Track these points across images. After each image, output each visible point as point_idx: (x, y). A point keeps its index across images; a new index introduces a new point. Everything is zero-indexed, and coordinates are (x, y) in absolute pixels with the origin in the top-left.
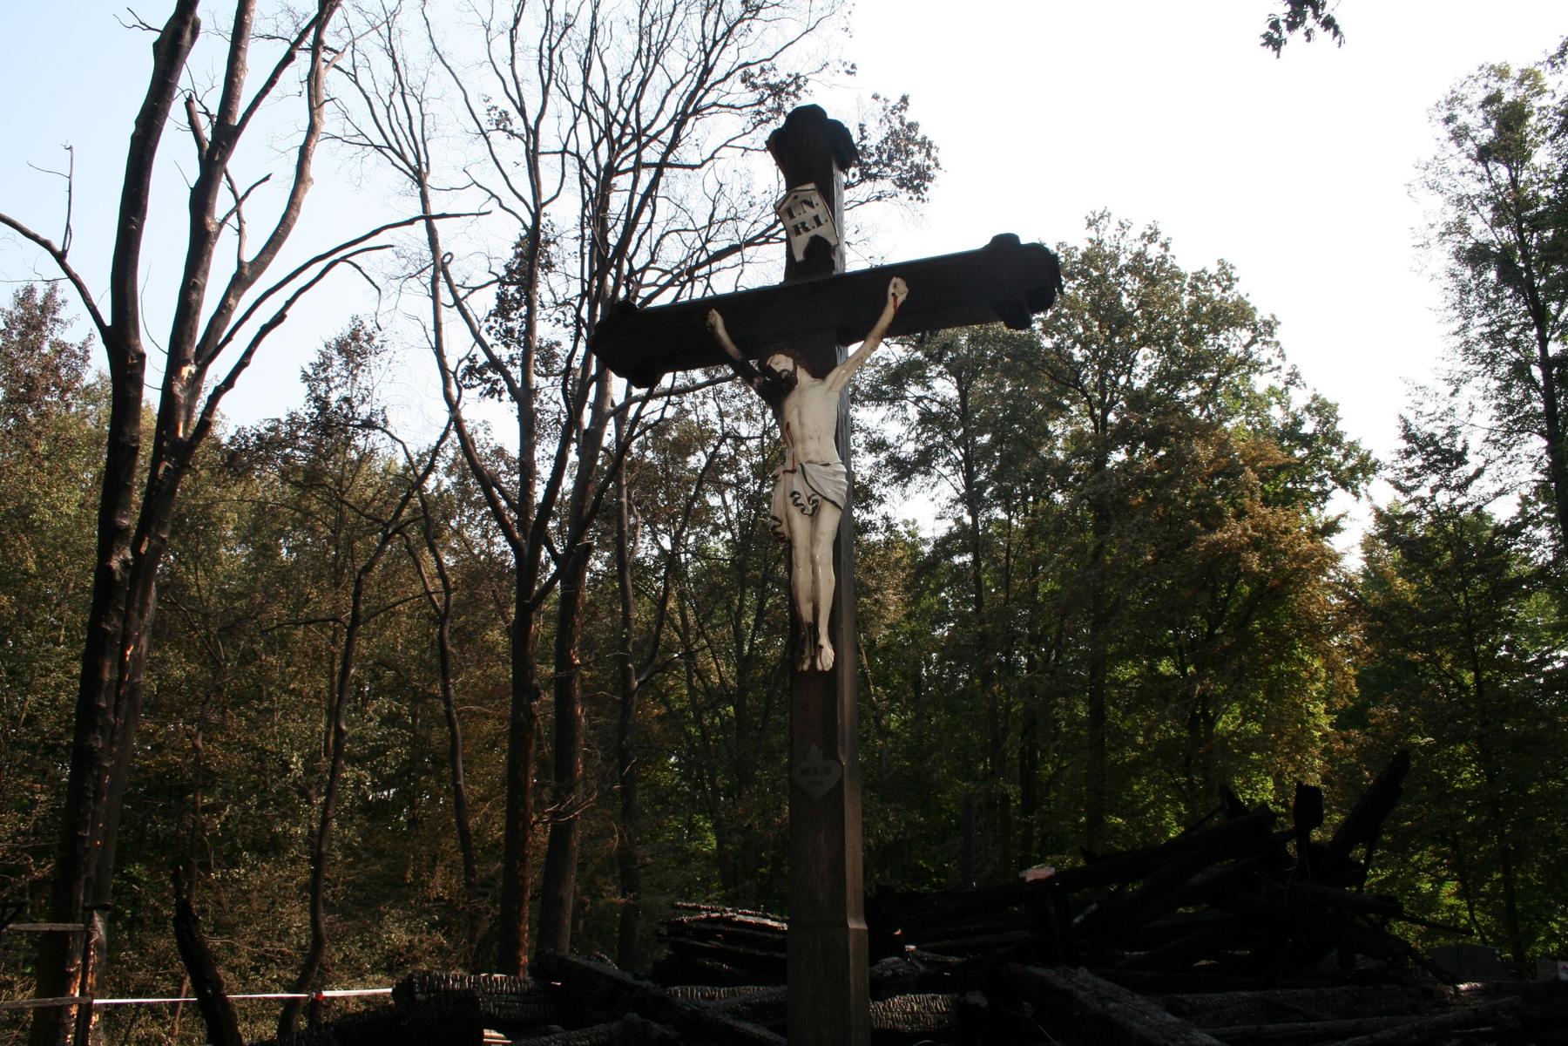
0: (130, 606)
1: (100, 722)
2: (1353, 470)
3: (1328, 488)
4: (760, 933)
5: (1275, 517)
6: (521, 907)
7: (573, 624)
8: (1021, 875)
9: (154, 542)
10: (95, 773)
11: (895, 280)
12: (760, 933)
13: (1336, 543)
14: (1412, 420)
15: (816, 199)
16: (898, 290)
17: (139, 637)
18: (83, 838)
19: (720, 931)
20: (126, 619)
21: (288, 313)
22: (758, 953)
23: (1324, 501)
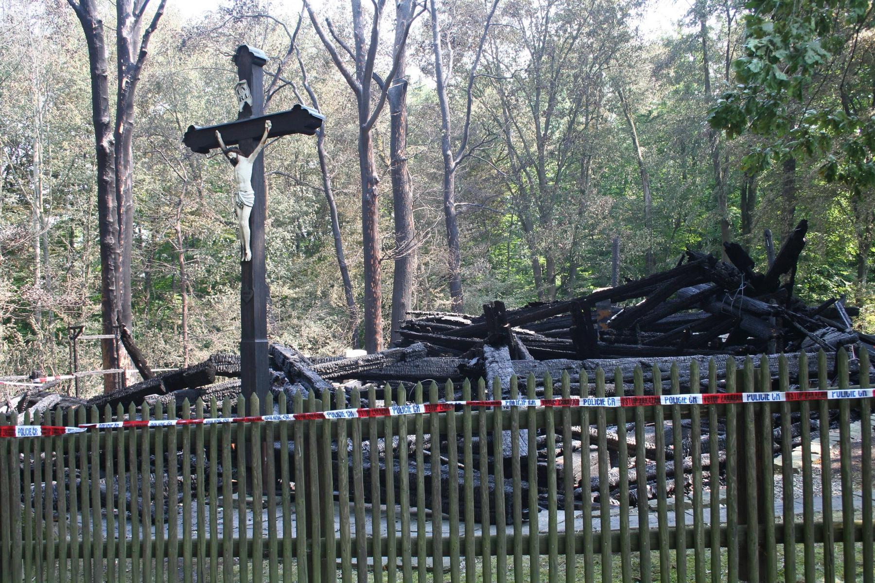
0: (117, 164)
1: (111, 230)
4: (449, 326)
6: (376, 310)
7: (400, 135)
9: (126, 126)
10: (113, 257)
11: (267, 121)
12: (449, 326)
15: (245, 86)
16: (268, 124)
17: (126, 180)
18: (112, 290)
19: (429, 326)
20: (117, 172)
22: (442, 337)
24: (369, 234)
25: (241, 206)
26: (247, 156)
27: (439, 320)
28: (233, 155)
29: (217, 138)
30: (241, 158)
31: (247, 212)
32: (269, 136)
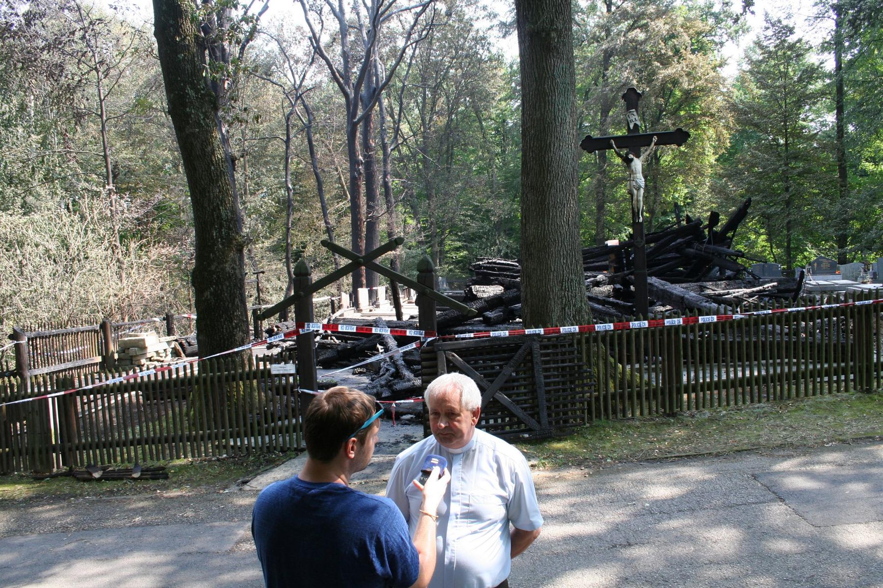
2: (737, 32)
3: (724, 40)
5: (696, 59)
8: (606, 242)
13: (724, 72)
14: (769, 12)
15: (635, 113)
16: (655, 139)
21: (269, 4)
23: (721, 47)
24: (356, 202)
25: (638, 189)
26: (638, 156)
27: (495, 263)
28: (631, 156)
29: (612, 144)
30: (635, 158)
31: (642, 191)
32: (655, 144)
